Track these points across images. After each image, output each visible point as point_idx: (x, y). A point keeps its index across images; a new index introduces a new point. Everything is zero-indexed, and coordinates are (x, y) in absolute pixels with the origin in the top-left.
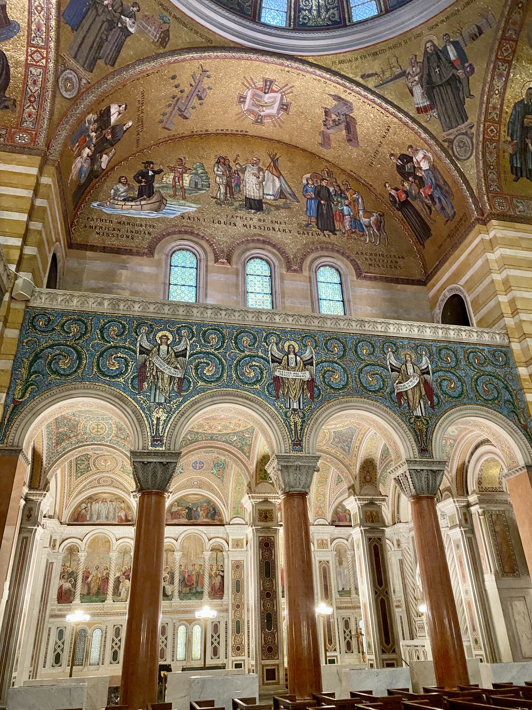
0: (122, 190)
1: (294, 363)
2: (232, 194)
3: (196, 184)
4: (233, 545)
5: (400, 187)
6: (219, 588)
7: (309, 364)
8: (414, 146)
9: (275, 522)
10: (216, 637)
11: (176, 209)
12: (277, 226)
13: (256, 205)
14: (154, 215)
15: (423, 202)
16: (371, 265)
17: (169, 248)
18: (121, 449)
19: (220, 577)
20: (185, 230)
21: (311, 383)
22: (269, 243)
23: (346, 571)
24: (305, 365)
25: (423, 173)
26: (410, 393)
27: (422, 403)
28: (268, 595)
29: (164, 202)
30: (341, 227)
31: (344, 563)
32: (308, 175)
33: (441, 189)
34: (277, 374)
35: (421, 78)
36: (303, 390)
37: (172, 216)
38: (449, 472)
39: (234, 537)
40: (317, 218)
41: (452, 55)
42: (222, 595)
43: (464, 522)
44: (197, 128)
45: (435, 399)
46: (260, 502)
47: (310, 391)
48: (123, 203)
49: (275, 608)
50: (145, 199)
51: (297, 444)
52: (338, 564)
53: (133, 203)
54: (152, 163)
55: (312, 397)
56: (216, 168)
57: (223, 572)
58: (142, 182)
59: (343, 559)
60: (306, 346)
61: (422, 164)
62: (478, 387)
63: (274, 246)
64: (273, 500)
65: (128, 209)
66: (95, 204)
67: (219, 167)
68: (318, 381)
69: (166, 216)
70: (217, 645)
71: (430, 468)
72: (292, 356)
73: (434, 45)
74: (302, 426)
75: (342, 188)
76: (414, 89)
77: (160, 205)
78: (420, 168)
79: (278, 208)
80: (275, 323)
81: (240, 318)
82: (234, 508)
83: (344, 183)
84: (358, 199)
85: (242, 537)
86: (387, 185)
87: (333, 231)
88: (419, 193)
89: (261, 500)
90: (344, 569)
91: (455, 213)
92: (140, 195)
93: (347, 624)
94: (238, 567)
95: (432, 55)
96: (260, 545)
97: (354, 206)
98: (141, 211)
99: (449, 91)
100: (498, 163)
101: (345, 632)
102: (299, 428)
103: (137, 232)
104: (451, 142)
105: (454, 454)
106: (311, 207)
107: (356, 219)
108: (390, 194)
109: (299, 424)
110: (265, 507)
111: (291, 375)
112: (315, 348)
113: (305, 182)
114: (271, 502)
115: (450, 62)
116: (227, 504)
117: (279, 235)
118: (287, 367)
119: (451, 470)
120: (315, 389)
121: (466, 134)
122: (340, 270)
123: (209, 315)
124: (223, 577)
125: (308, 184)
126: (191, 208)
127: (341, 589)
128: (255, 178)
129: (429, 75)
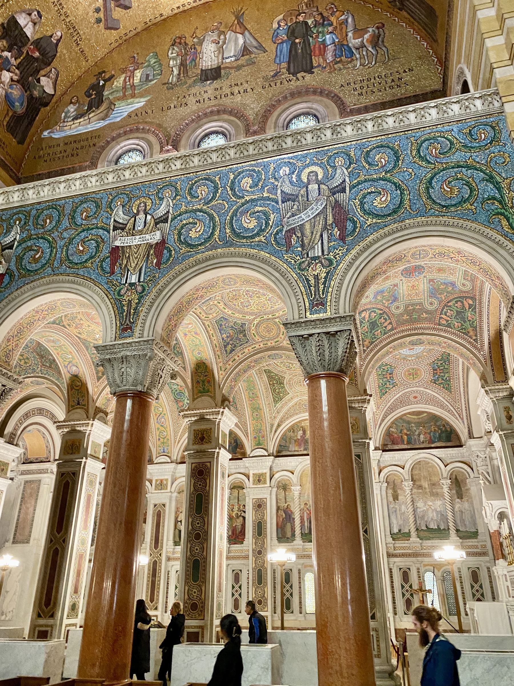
0: (72, 110)
1: (143, 224)
2: (186, 72)
3: (148, 76)
4: (254, 481)
6: (241, 531)
7: (162, 222)
9: (213, 444)
10: (237, 587)
11: (123, 110)
12: (236, 90)
13: (214, 74)
14: (102, 124)
16: (361, 94)
17: (113, 153)
18: (51, 378)
19: (241, 518)
20: (131, 127)
21: (161, 246)
22: (225, 112)
23: (403, 507)
24: (156, 224)
26: (308, 226)
27: (325, 236)
28: (198, 537)
29: (113, 107)
31: (400, 497)
32: (281, 17)
34: (117, 243)
36: (148, 258)
37: (118, 119)
38: (479, 351)
39: (256, 472)
40: (289, 63)
42: (243, 539)
43: (504, 421)
44: (150, 16)
45: (349, 226)
46: (196, 421)
47: (157, 257)
48: (72, 123)
49: (205, 553)
50: (93, 111)
51: (125, 327)
52: (391, 499)
53: (82, 120)
54: (104, 72)
55: (158, 264)
56: (170, 52)
57: (245, 512)
58: (92, 95)
59: (399, 492)
60: (161, 199)
62: (431, 190)
63: (231, 113)
64: (211, 417)
65: (76, 127)
66: (46, 133)
67: (174, 49)
68: (172, 240)
69: (113, 121)
70: (239, 598)
71: (325, 330)
72: (142, 216)
75: (325, 14)
77: (108, 112)
79: (238, 68)
80: (125, 180)
81: (82, 187)
82: (255, 438)
83: (328, 8)
84: (347, 20)
85: (264, 471)
87: (310, 70)
89: (196, 418)
90: (400, 506)
92: (90, 108)
93: (405, 576)
94: (259, 506)
96: (192, 473)
97: (341, 30)
98: (91, 124)
101: (403, 587)
103: (82, 147)
105: (481, 321)
106: (281, 52)
107: (343, 45)
110: (203, 426)
111: (136, 241)
113: (275, 26)
114: (209, 420)
116: (247, 434)
117: (238, 99)
119: (482, 346)
120: (165, 251)
122: (317, 114)
123: (46, 194)
124: (244, 518)
125: (280, 26)
126: (139, 103)
127: (396, 530)
128: (214, 45)
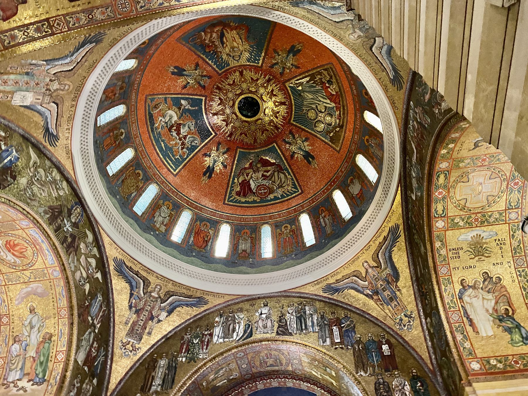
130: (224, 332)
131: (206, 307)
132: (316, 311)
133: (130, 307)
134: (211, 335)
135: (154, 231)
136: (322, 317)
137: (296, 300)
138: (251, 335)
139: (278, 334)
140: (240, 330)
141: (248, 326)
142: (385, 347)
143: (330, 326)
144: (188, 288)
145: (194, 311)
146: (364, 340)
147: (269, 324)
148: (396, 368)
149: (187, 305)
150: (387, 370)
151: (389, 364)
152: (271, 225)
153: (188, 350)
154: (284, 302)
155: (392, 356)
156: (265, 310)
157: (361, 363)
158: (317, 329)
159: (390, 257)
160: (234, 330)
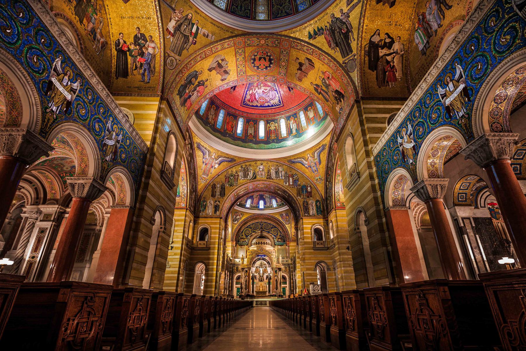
5: (128, 43)
8: (153, 39)
15: (135, 62)
25: (147, 52)
30: (86, 24)
33: (150, 67)
35: (178, 21)
41: (194, 30)
61: (149, 49)
73: (192, 18)
74: (52, 123)
76: (172, 21)
78: (147, 49)
86: (121, 35)
88: (136, 57)
91: (149, 82)
95: (188, 19)
99: (183, 39)
100: (178, 83)
102: (50, 123)
104: (169, 56)
108: (119, 40)
109: (51, 121)
112: (81, 86)
115: (191, 31)
118: (61, 81)
121: (176, 60)
129: (181, 24)
130: (244, 175)
131: (235, 162)
132: (283, 170)
133: (203, 162)
134: (238, 175)
135: (209, 124)
136: (286, 173)
137: (275, 163)
138: (255, 177)
139: (267, 178)
140: (251, 174)
141: (254, 173)
142: (309, 188)
143: (289, 177)
144: (227, 154)
145: (230, 164)
146: (302, 185)
147: (263, 174)
148: (311, 196)
149: (227, 161)
150: (308, 197)
151: (309, 195)
152: (264, 121)
153: (229, 182)
154: (270, 164)
155: (311, 192)
156: (261, 167)
157: (299, 194)
158: (283, 178)
159: (319, 155)
160: (248, 174)
